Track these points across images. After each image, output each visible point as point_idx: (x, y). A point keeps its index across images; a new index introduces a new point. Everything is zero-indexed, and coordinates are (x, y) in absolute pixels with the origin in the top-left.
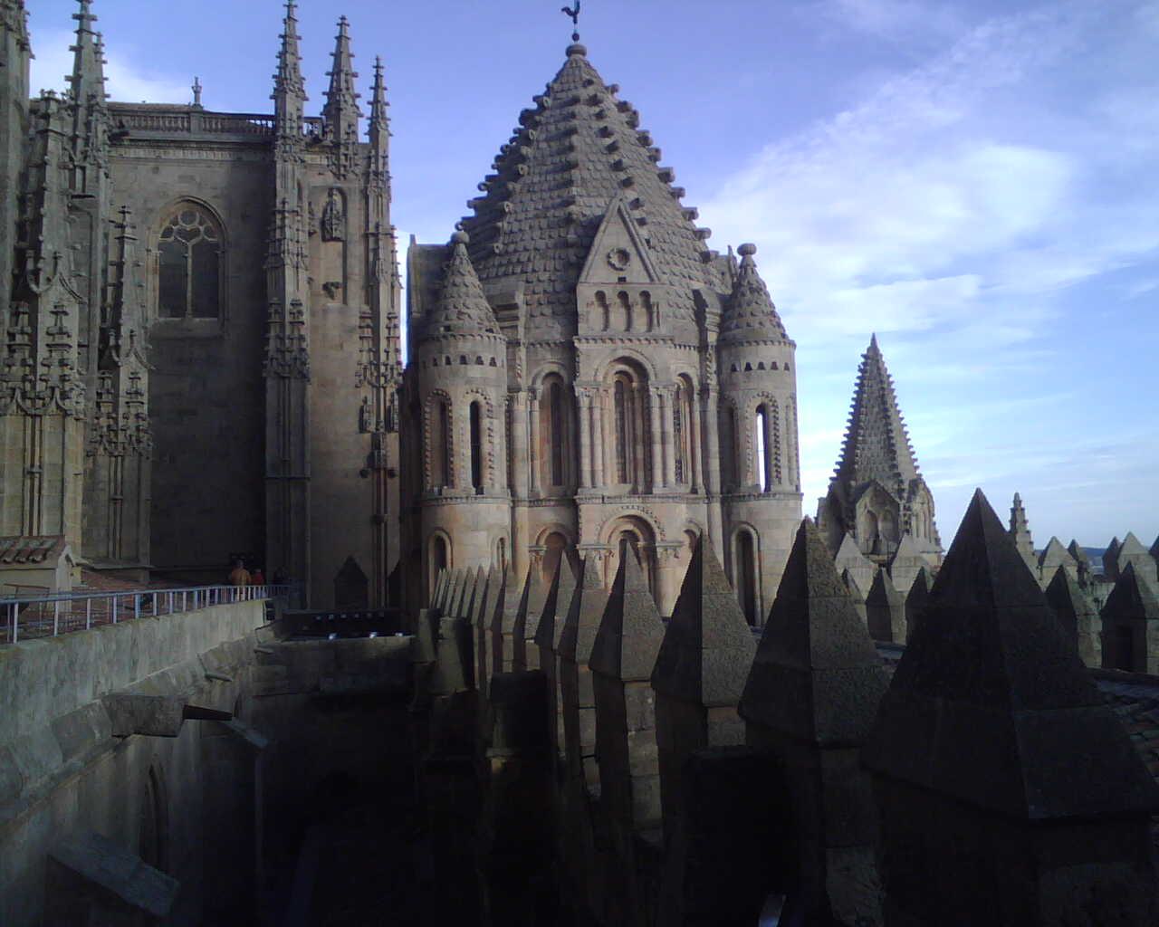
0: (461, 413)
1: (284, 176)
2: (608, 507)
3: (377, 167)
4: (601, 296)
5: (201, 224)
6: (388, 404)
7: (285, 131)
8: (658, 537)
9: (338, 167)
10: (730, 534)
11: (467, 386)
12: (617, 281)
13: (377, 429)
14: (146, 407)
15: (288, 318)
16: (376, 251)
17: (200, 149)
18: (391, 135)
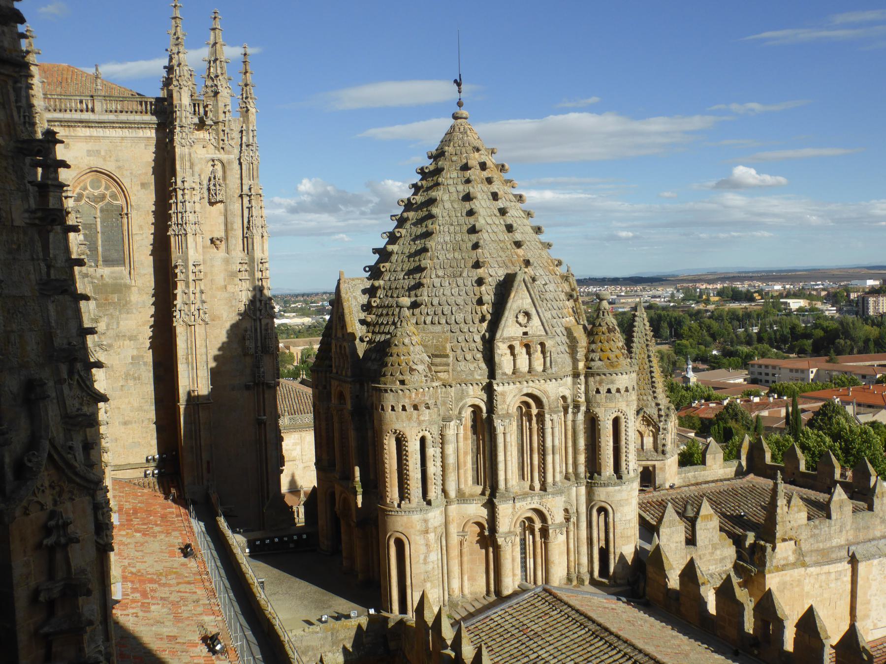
0: (413, 447)
1: (182, 158)
3: (248, 140)
4: (511, 348)
5: (107, 188)
6: (263, 332)
7: (181, 121)
8: (550, 522)
9: (218, 140)
12: (521, 335)
13: (256, 352)
15: (192, 277)
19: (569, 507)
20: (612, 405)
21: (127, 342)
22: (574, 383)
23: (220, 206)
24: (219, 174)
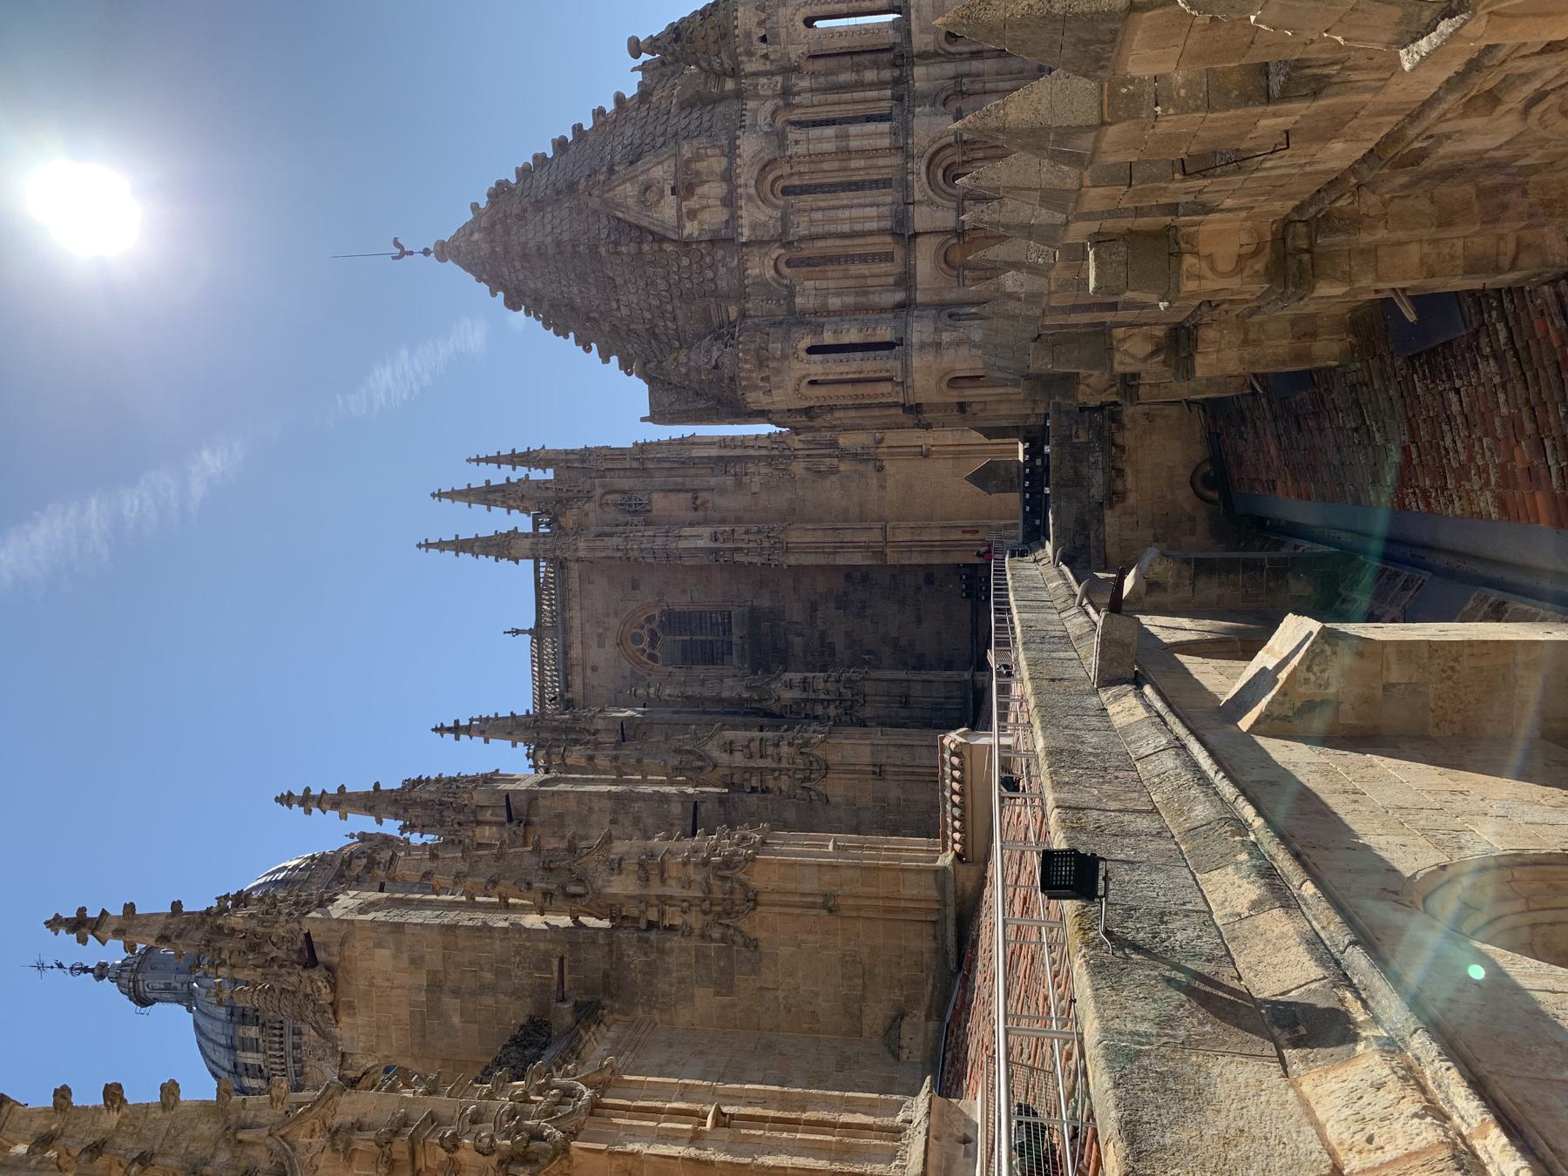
2: (918, 196)
4: (692, 214)
5: (642, 627)
9: (579, 499)
10: (949, 53)
11: (791, 358)
12: (674, 197)
14: (817, 674)
16: (660, 460)
17: (571, 627)
18: (544, 447)
19: (943, 96)
20: (783, 35)
21: (819, 614)
22: (757, 96)
23: (655, 496)
24: (617, 497)
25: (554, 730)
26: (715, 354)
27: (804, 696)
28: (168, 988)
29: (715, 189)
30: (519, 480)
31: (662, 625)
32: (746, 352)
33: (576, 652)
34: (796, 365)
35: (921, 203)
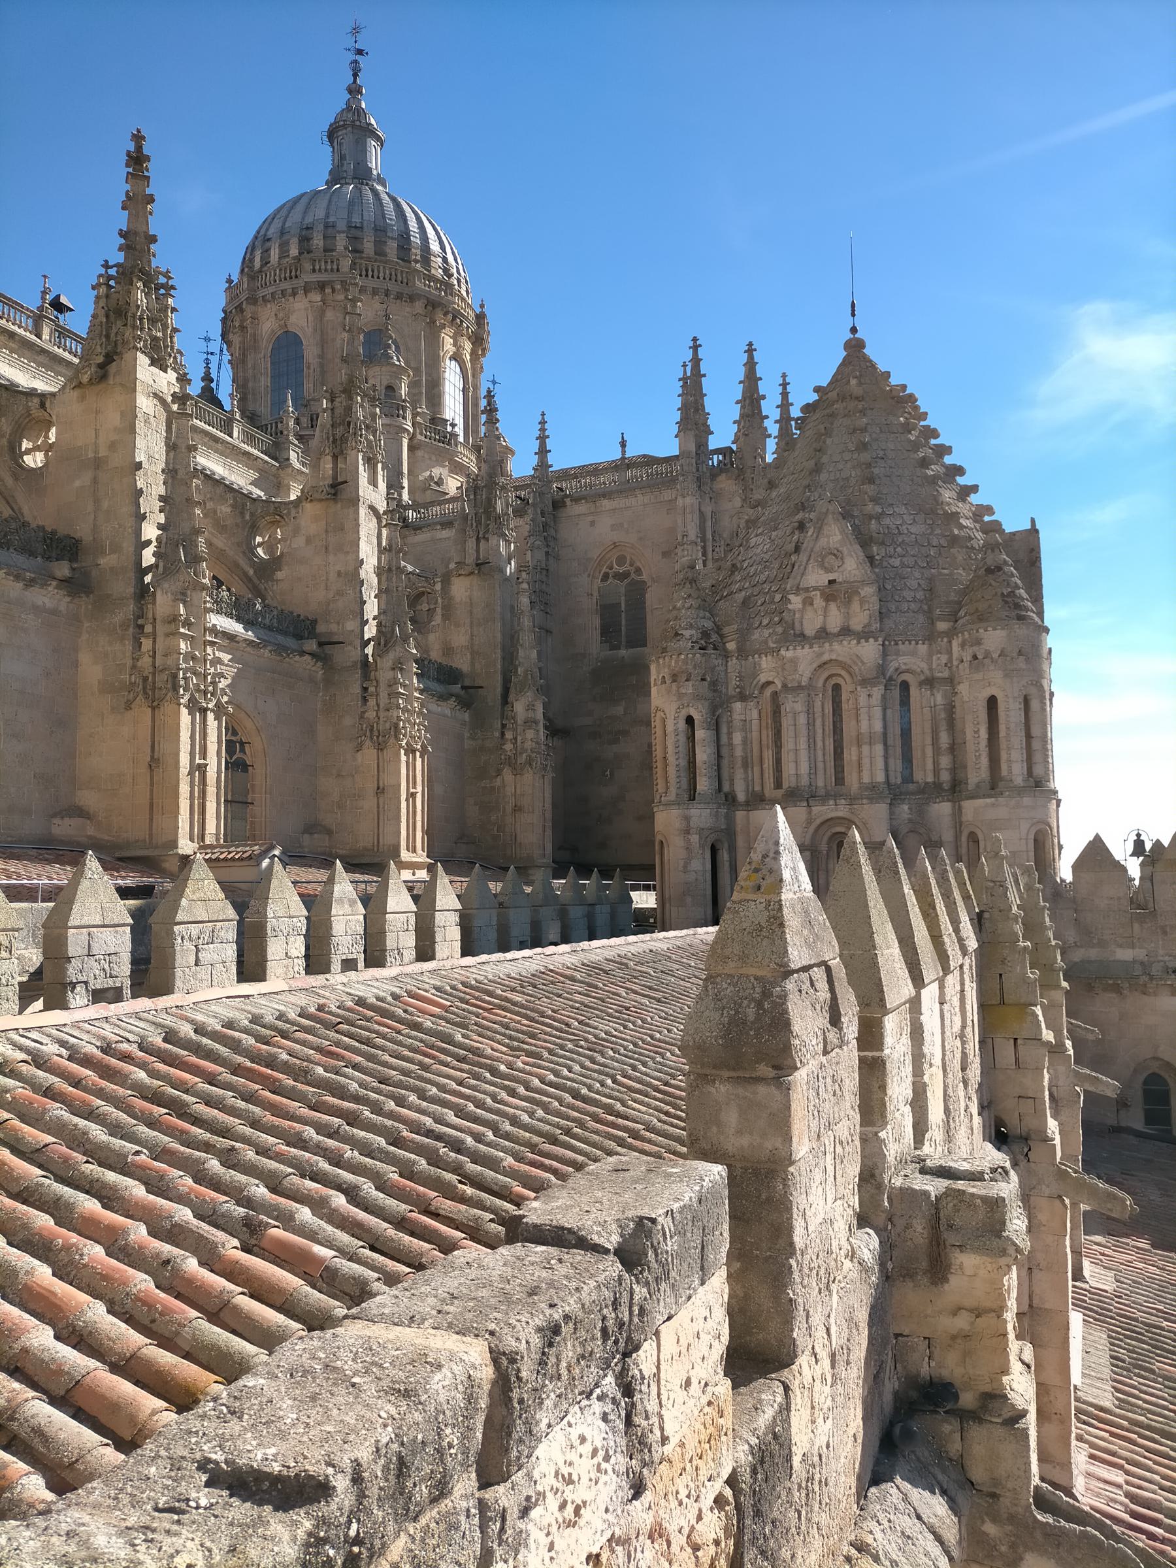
2: (816, 810)
5: (631, 565)
19: (922, 831)
25: (489, 500)
26: (687, 633)
27: (519, 722)
28: (342, 158)
29: (835, 621)
30: (766, 429)
31: (634, 583)
32: (685, 662)
33: (606, 504)
34: (674, 706)
35: (810, 813)
